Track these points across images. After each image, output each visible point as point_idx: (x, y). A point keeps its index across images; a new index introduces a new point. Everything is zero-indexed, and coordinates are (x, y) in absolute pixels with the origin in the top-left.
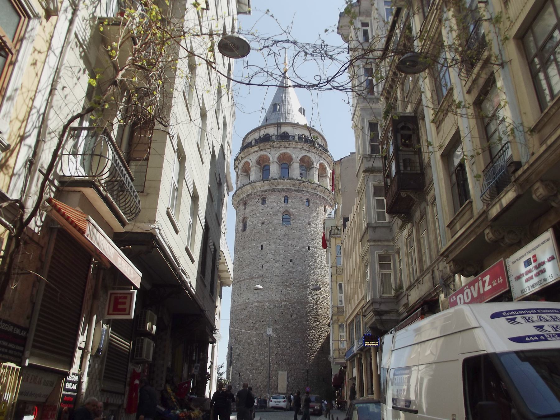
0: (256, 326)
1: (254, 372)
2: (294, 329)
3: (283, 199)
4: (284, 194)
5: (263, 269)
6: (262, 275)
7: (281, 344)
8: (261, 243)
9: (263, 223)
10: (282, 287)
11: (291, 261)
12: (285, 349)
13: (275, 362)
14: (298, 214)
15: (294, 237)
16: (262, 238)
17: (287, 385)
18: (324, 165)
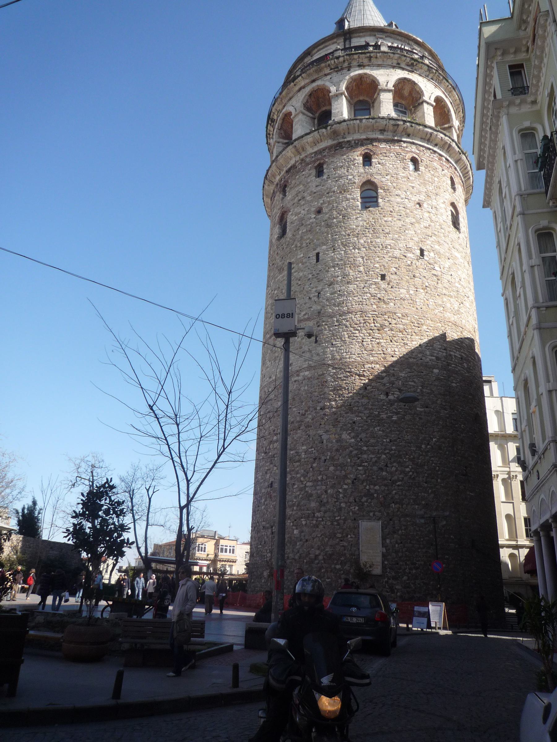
0: (307, 420)
1: (304, 523)
2: (395, 422)
3: (361, 158)
4: (361, 150)
5: (321, 299)
6: (319, 313)
7: (365, 456)
8: (314, 249)
9: (319, 212)
10: (364, 331)
11: (383, 277)
12: (375, 468)
13: (352, 499)
14: (395, 185)
15: (387, 231)
16: (318, 240)
17: (384, 556)
18: (445, 106)
